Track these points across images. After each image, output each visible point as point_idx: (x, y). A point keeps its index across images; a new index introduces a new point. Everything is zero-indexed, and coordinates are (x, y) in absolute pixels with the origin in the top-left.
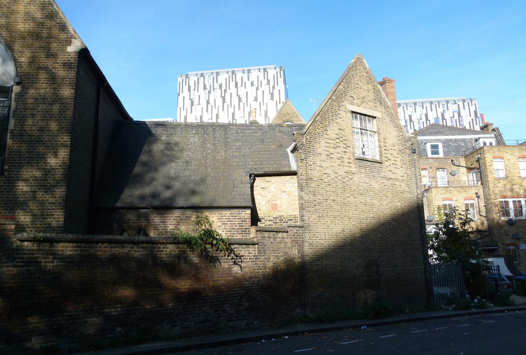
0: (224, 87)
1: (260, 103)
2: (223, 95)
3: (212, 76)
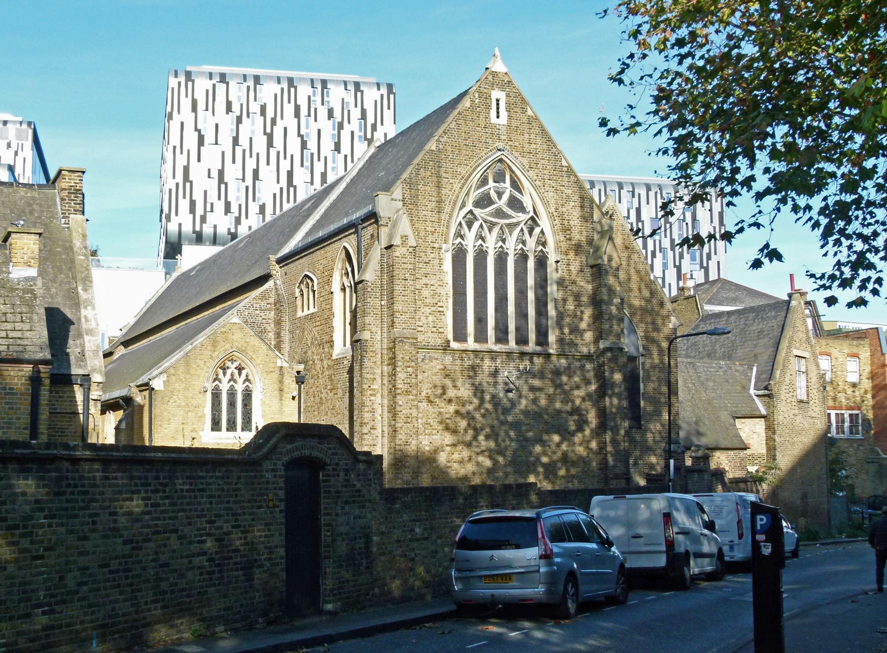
0: (270, 114)
1: (346, 156)
2: (268, 131)
3: (245, 84)
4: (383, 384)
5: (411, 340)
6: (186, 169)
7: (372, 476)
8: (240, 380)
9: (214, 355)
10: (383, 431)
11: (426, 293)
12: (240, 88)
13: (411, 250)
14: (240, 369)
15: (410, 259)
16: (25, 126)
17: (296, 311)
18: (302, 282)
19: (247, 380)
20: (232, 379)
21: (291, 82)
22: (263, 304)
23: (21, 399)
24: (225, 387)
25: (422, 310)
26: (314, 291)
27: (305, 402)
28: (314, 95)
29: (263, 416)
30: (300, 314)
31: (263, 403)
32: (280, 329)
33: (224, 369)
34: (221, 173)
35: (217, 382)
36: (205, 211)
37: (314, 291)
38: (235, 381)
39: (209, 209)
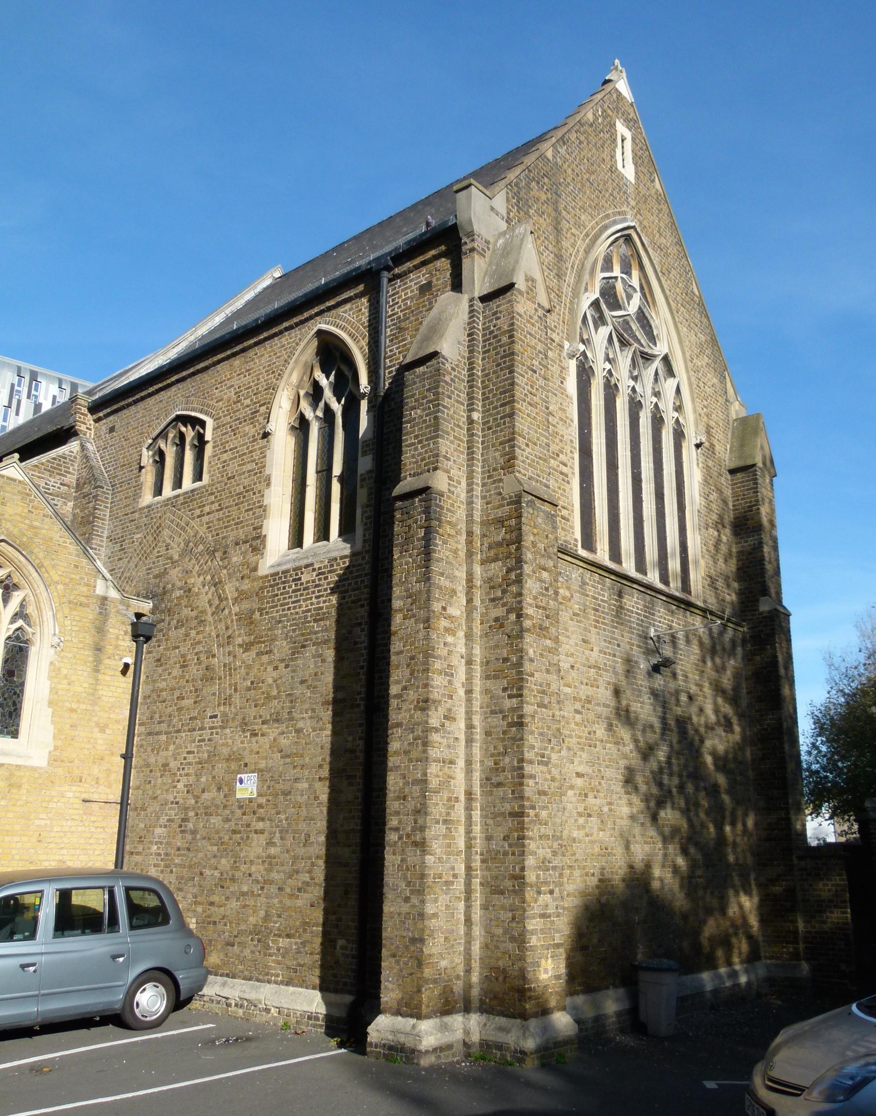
10: (470, 727)
18: (163, 434)
19: (21, 614)
29: (51, 703)
30: (147, 498)
31: (55, 672)
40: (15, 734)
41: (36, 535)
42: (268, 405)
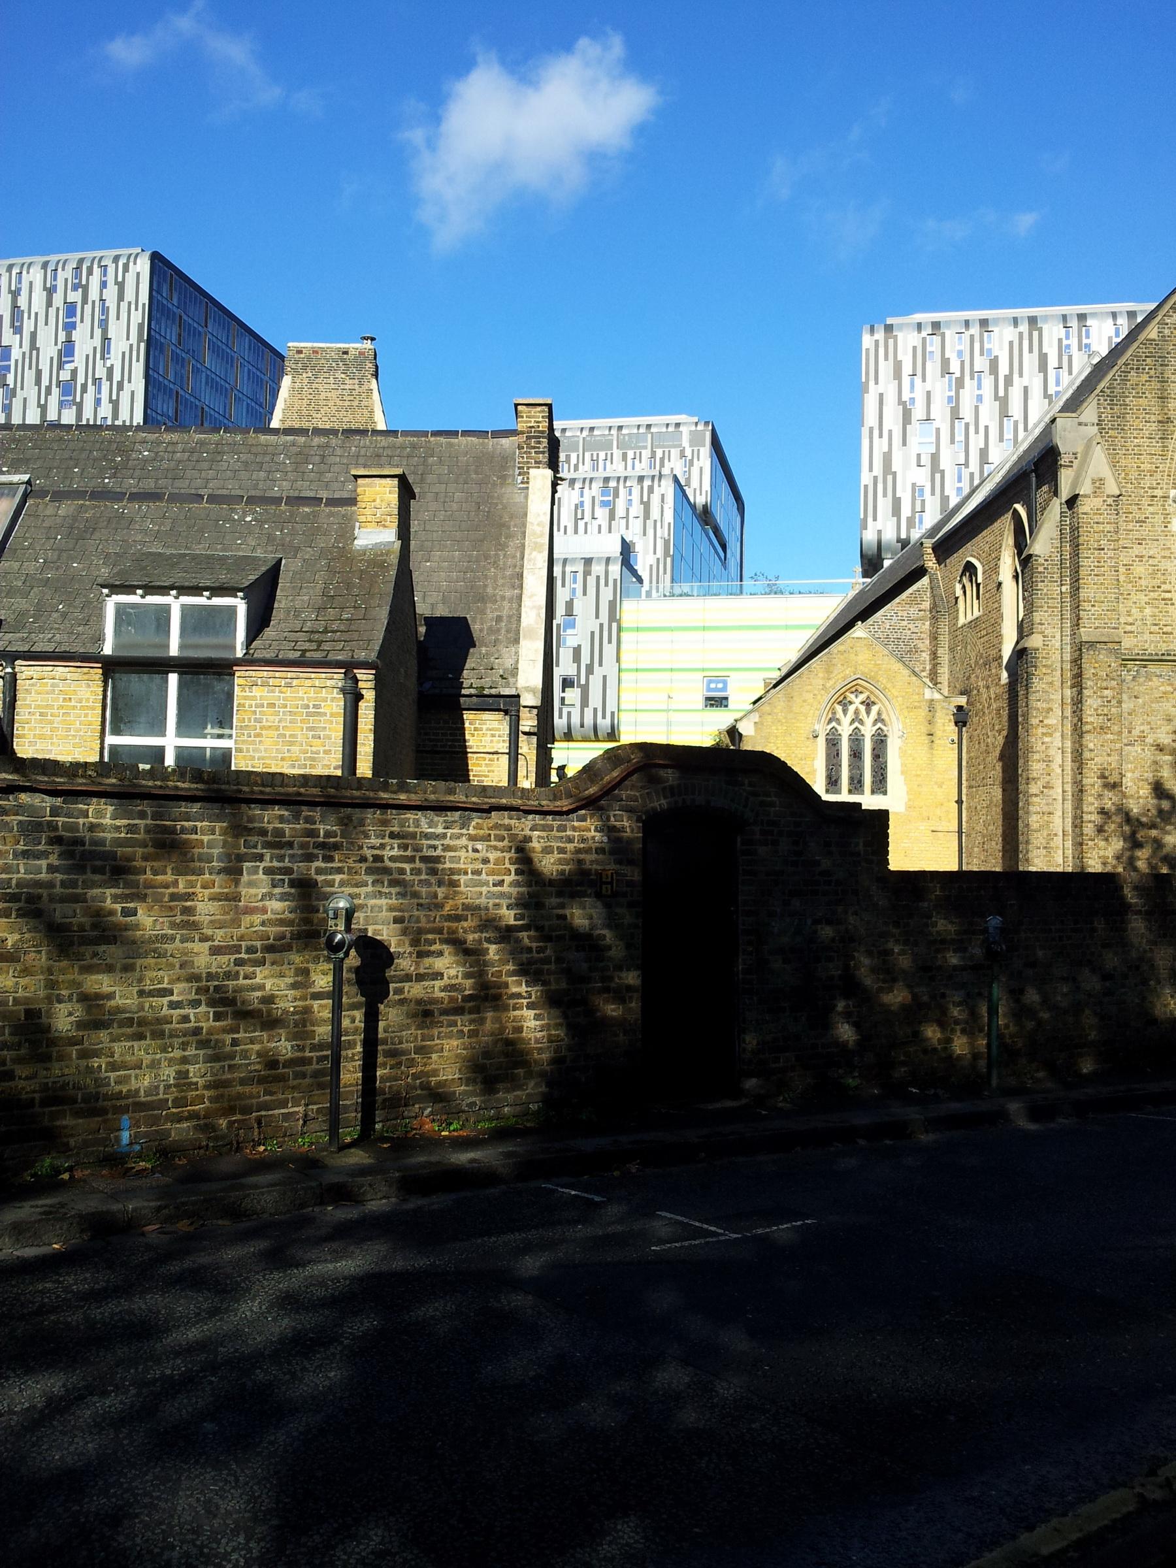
0: (1003, 370)
3: (968, 333)
4: (1063, 718)
5: (1110, 646)
6: (887, 458)
7: (861, 848)
8: (869, 721)
9: (828, 685)
11: (1139, 569)
12: (960, 339)
13: (1110, 501)
14: (868, 705)
15: (1107, 516)
16: (701, 427)
17: (957, 618)
19: (879, 719)
20: (857, 718)
21: (1033, 321)
22: (913, 611)
23: (331, 723)
24: (845, 730)
25: (1134, 597)
26: (978, 585)
27: (968, 752)
28: (1067, 338)
29: (902, 773)
30: (962, 621)
31: (903, 752)
32: (936, 646)
33: (845, 704)
34: (935, 458)
35: (834, 724)
36: (914, 511)
37: (978, 585)
38: (861, 722)
39: (918, 508)
40: (885, 793)
41: (880, 669)
42: (997, 566)
